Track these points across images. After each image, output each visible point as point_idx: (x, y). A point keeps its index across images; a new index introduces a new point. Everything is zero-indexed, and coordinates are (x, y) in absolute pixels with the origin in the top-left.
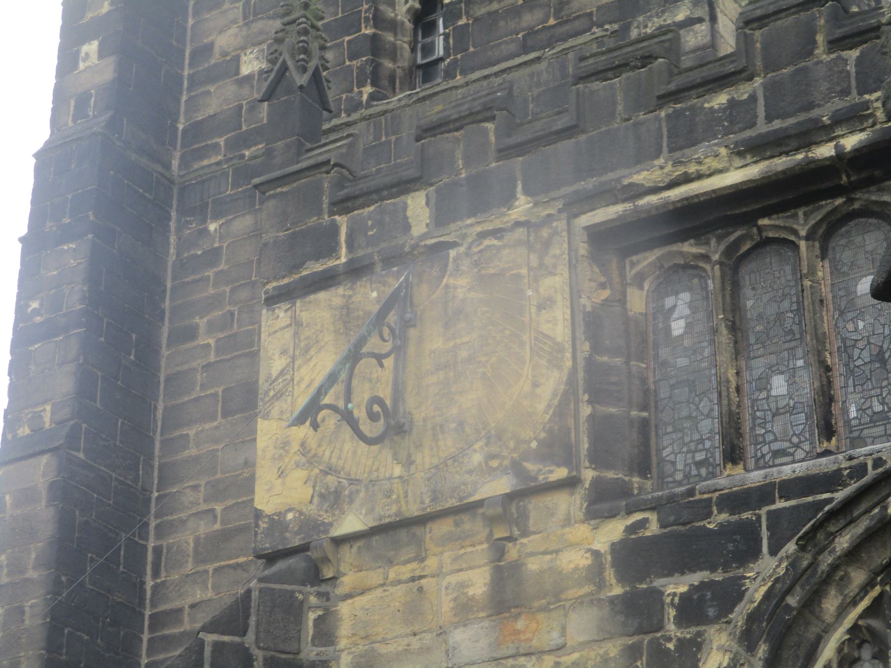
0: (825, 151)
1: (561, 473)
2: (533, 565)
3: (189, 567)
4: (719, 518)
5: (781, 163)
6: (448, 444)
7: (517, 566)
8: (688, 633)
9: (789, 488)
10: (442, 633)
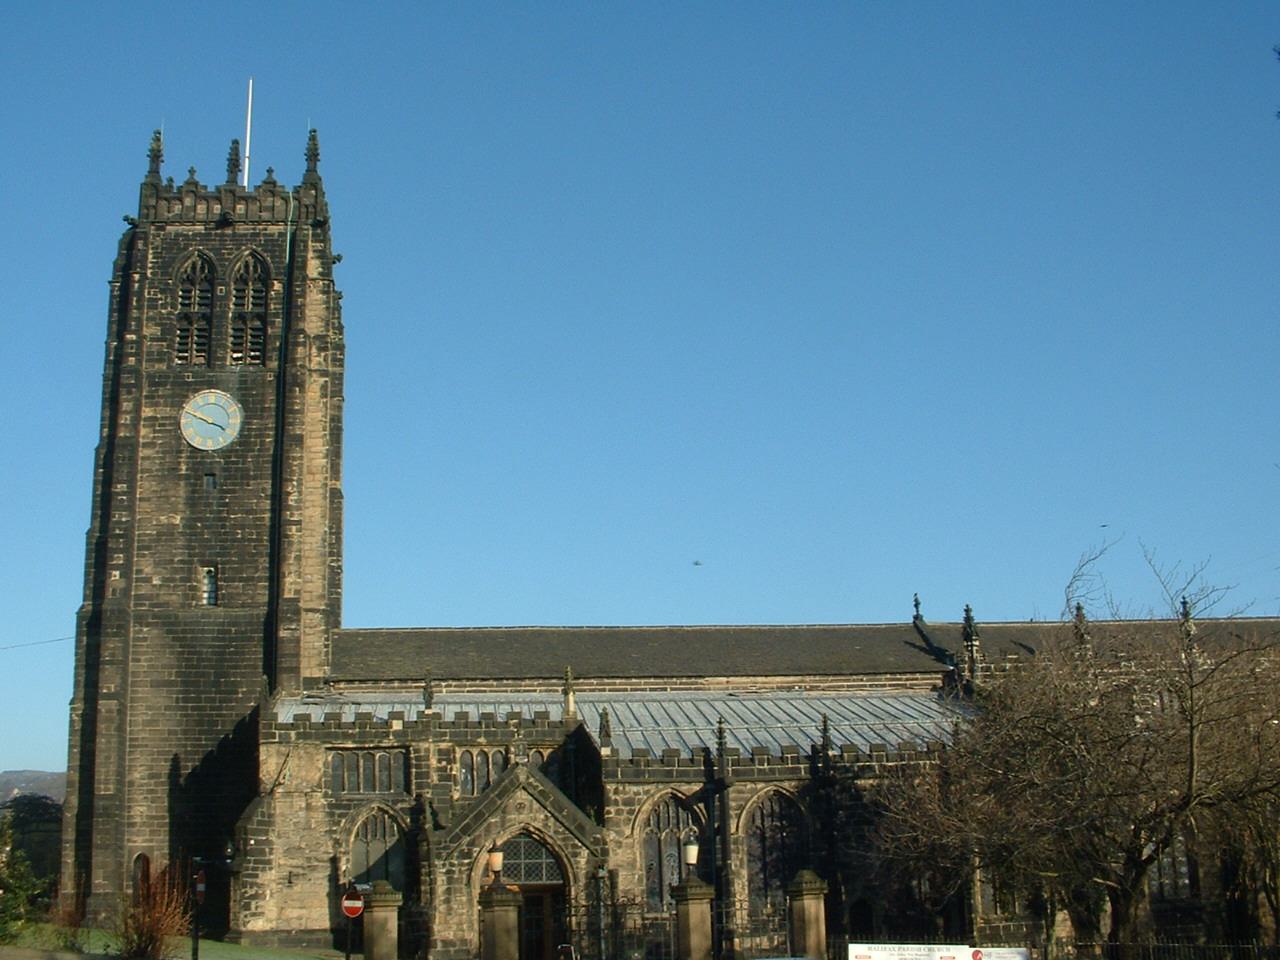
0: (367, 746)
2: (314, 804)
3: (140, 728)
4: (345, 802)
5: (359, 745)
6: (299, 781)
9: (358, 800)
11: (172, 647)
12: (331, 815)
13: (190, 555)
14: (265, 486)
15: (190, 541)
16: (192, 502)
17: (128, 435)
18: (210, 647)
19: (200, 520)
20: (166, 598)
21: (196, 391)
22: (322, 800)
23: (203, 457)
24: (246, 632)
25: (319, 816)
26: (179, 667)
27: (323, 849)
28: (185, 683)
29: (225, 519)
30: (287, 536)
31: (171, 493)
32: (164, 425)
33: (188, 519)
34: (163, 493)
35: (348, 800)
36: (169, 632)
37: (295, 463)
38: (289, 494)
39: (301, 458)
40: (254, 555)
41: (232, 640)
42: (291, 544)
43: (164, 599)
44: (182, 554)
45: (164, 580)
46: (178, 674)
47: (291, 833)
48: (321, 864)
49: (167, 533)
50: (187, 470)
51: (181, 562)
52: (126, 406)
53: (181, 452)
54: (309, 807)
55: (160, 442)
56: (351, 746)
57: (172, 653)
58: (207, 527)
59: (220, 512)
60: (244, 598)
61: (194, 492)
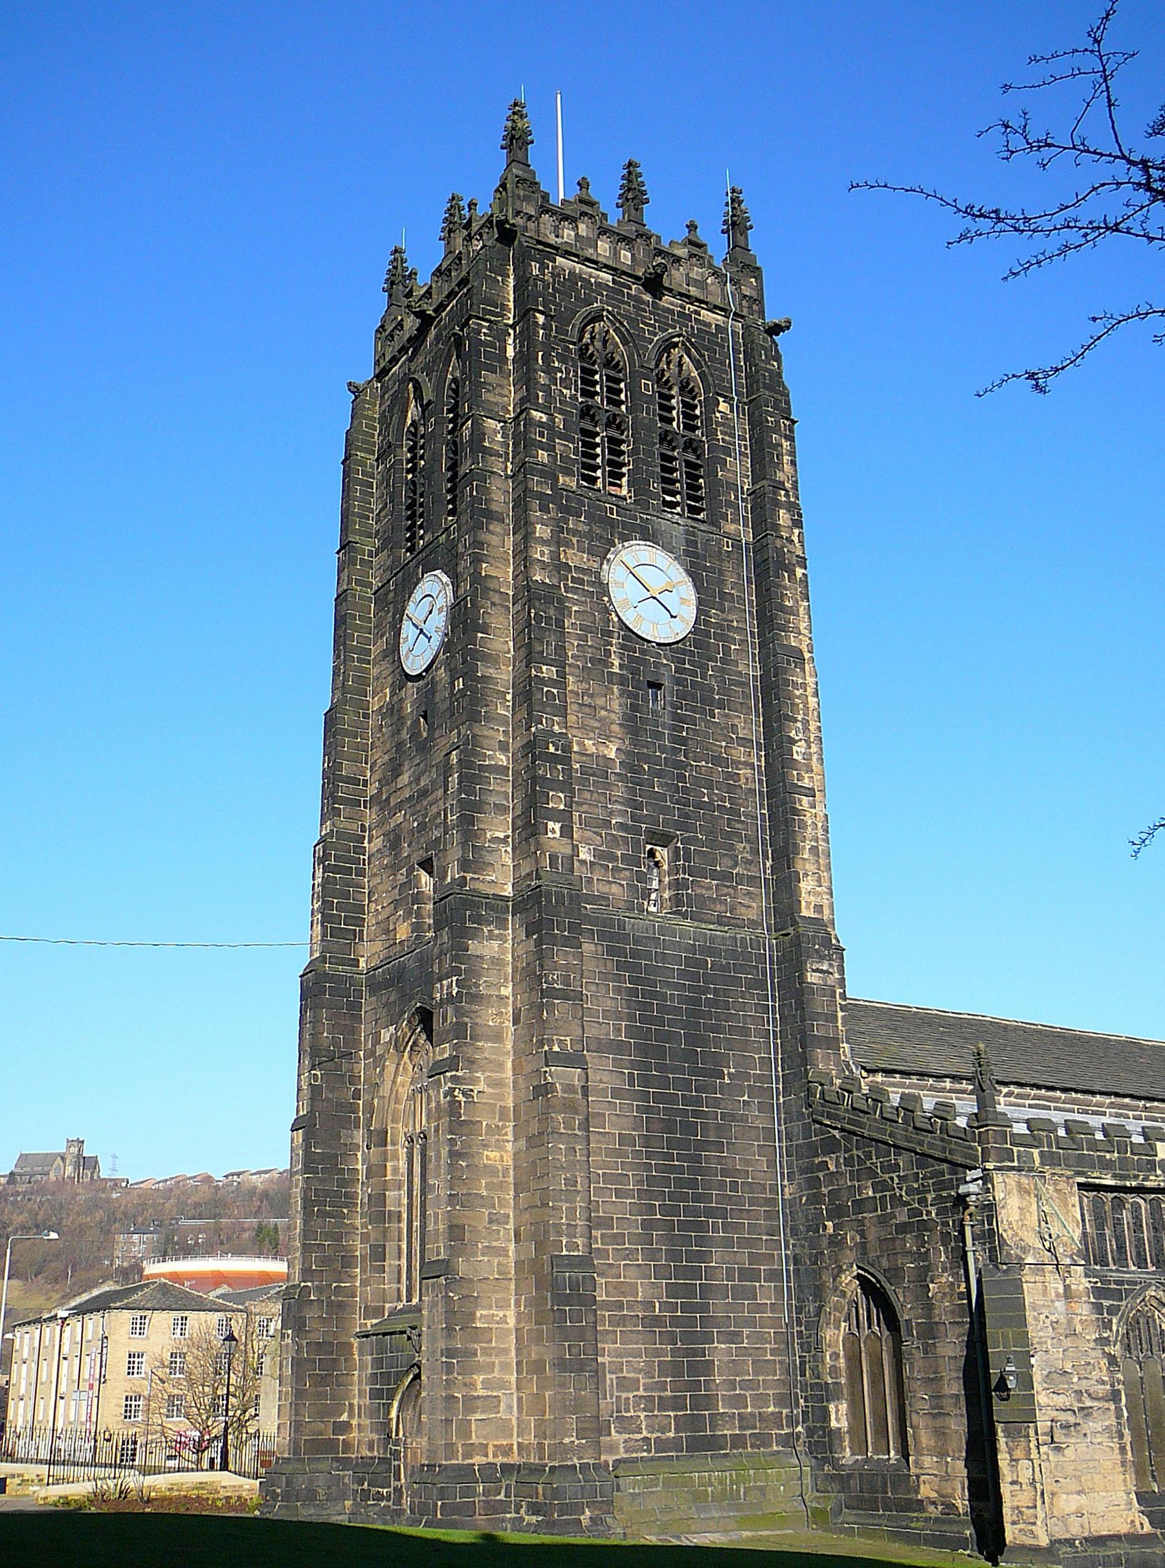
1: (1083, 1262)
2: (1073, 1287)
7: (1069, 1286)
8: (1109, 1317)
10: (1052, 1301)
11: (618, 979)
12: (1098, 1308)
13: (633, 817)
14: (736, 721)
15: (632, 791)
16: (634, 724)
17: (547, 581)
18: (676, 986)
19: (647, 759)
20: (605, 889)
21: (625, 538)
22: (1084, 1280)
23: (642, 652)
24: (726, 968)
25: (1084, 1309)
26: (631, 1017)
27: (1095, 1375)
28: (643, 1050)
29: (685, 766)
30: (796, 812)
31: (600, 702)
32: (581, 582)
33: (628, 753)
34: (587, 700)
35: (1117, 1282)
36: (611, 951)
37: (797, 693)
38: (793, 742)
39: (804, 686)
40: (728, 836)
41: (707, 979)
42: (803, 825)
43: (598, 888)
44: (623, 813)
45: (598, 854)
46: (631, 1031)
47: (1049, 1342)
48: (1096, 1404)
49: (598, 770)
50: (621, 666)
51: (622, 826)
52: (541, 531)
53: (610, 634)
54: (1068, 1294)
55: (575, 608)
56: (1112, 1182)
57: (618, 990)
58: (659, 774)
59: (676, 751)
60: (719, 907)
61: (634, 708)
